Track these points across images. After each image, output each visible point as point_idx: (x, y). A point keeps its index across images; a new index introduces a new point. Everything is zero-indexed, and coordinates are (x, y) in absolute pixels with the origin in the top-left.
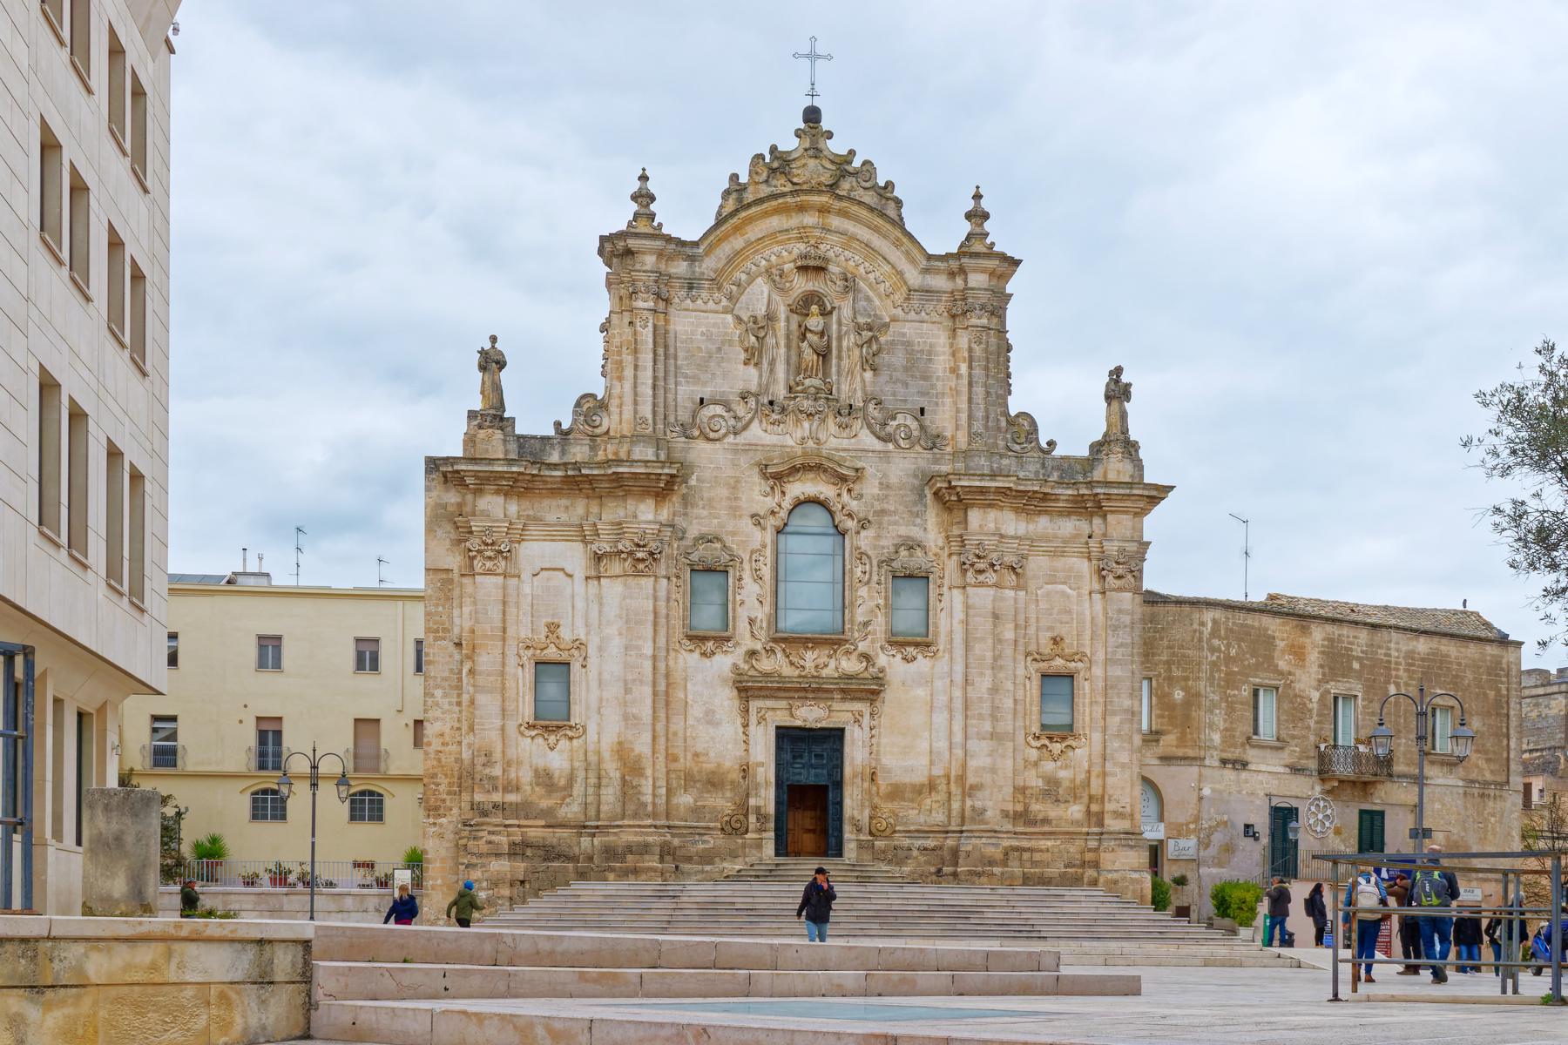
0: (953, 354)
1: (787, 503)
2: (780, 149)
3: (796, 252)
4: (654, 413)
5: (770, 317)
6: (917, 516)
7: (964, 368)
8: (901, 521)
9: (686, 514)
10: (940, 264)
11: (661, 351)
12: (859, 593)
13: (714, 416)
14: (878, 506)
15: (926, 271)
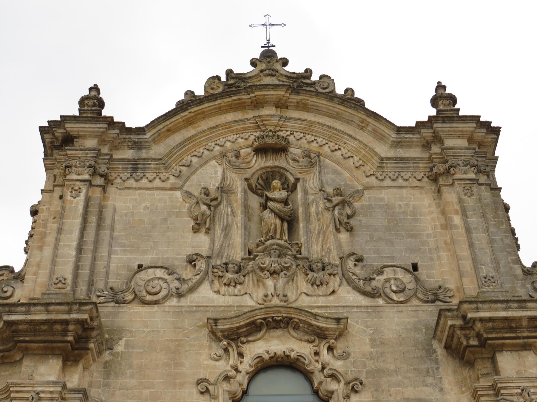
0: (443, 213)
1: (246, 365)
3: (252, 137)
4: (76, 276)
6: (428, 374)
7: (457, 220)
8: (406, 381)
9: (106, 385)
10: (411, 136)
11: (93, 219)
13: (152, 279)
14: (371, 365)
15: (397, 144)
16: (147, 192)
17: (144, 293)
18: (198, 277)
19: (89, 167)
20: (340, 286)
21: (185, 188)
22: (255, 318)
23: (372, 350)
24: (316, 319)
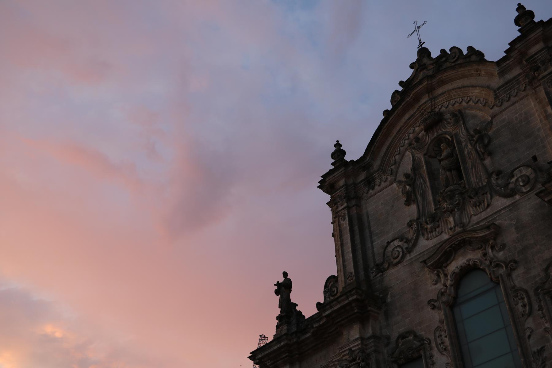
2: (404, 80)
5: (416, 168)
10: (508, 62)
11: (356, 228)
12: (526, 326)
13: (393, 249)
16: (380, 193)
17: (392, 260)
18: (415, 235)
19: (344, 198)
20: (491, 198)
21: (397, 180)
22: (445, 249)
23: (518, 235)
24: (476, 233)
